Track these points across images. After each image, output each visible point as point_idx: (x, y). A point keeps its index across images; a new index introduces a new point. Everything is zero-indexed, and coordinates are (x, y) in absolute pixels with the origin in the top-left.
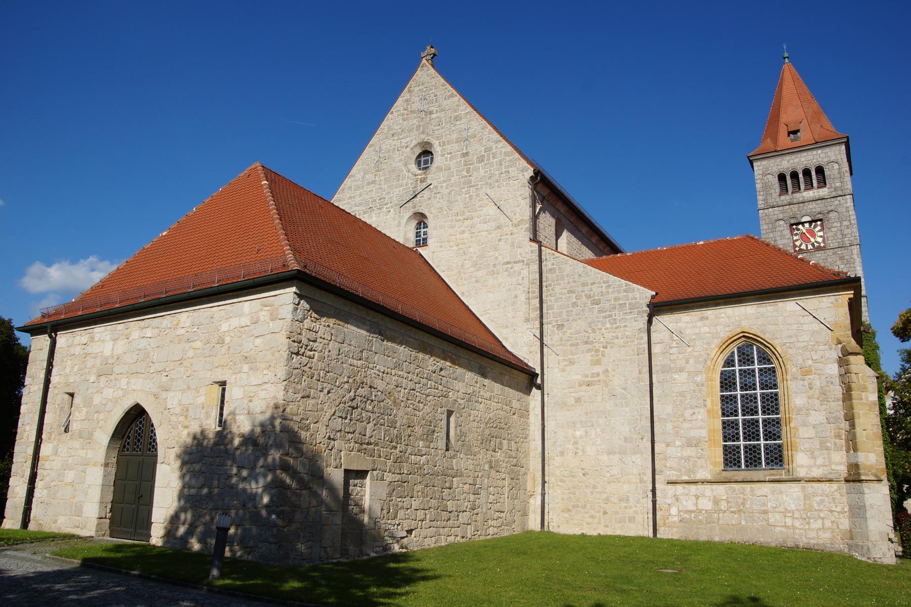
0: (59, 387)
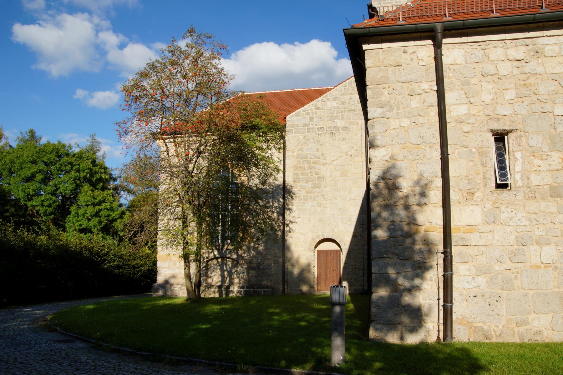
0: (472, 120)
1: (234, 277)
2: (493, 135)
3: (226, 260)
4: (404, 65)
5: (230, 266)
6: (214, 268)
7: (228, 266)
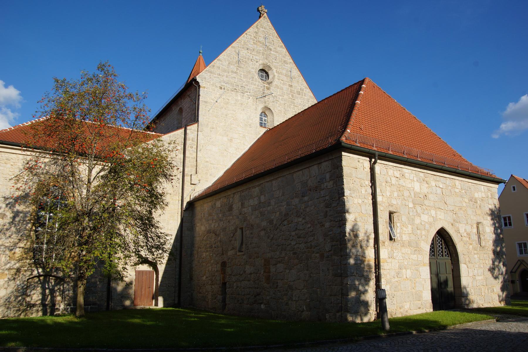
1: (56, 294)
2: (389, 213)
3: (49, 279)
4: (358, 169)
5: (53, 284)
6: (35, 286)
7: (50, 284)
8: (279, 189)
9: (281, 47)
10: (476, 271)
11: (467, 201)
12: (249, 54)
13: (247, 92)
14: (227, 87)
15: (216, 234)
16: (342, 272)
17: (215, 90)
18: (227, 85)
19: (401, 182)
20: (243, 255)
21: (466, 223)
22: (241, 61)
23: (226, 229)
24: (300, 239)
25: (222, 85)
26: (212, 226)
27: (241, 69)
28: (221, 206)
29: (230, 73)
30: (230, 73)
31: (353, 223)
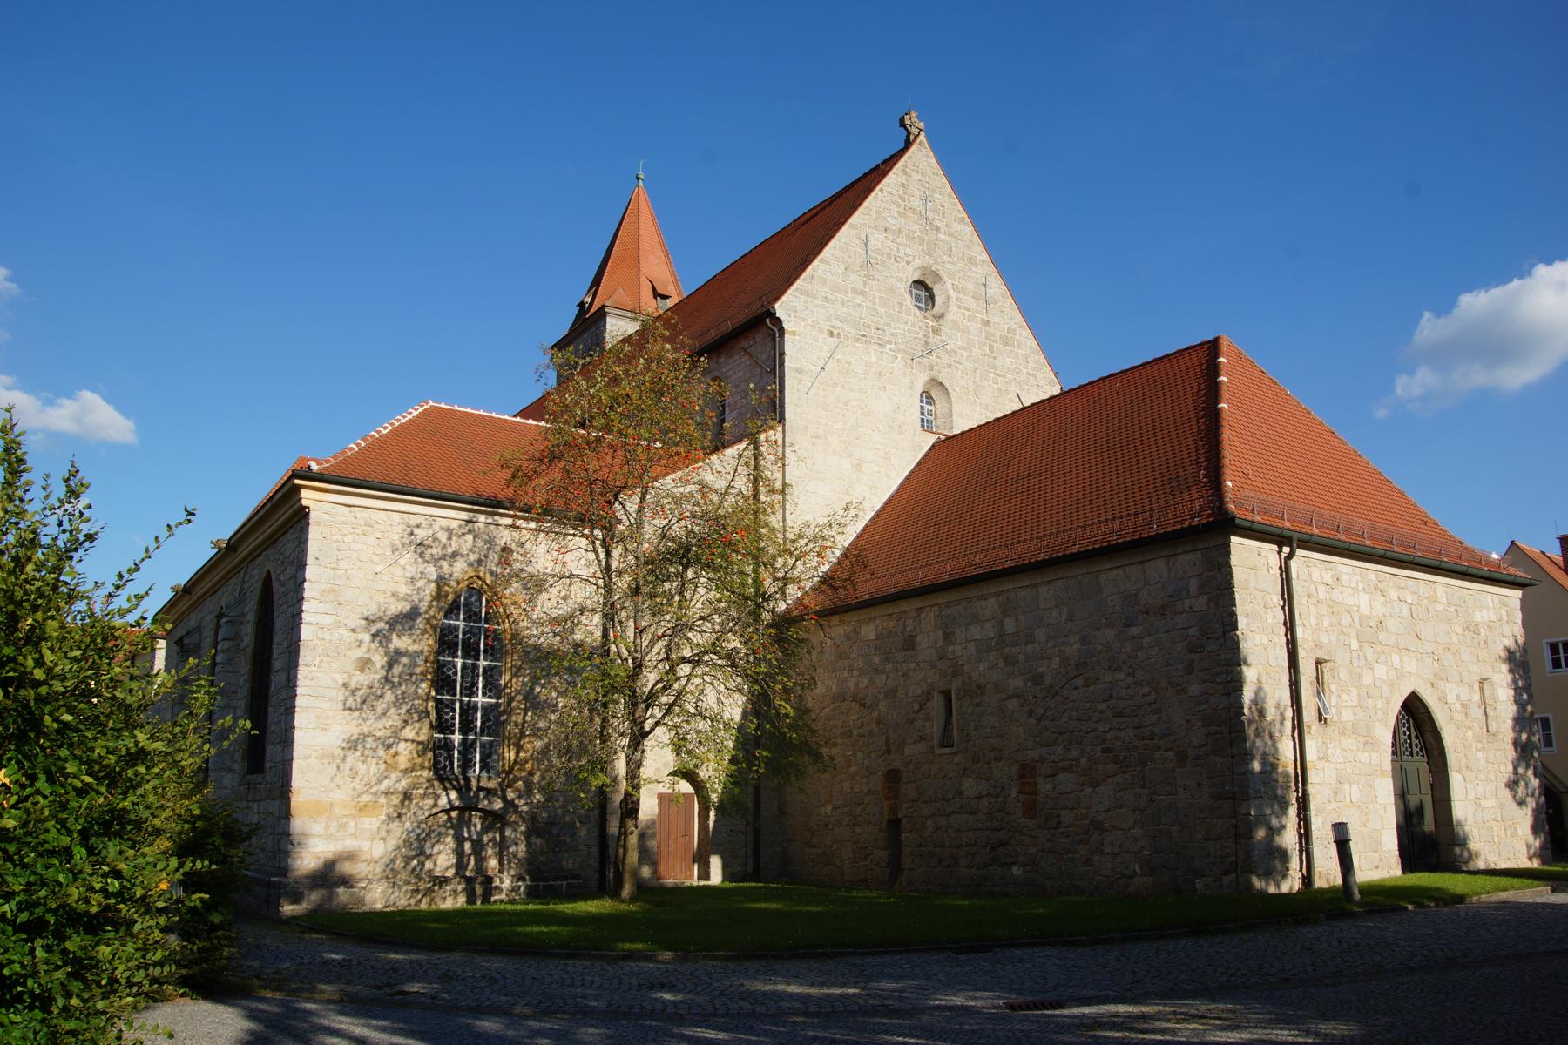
3: (471, 816)
5: (479, 827)
6: (440, 834)
7: (473, 829)
8: (1056, 606)
9: (961, 221)
10: (1480, 788)
11: (1459, 629)
12: (889, 243)
13: (890, 343)
14: (843, 331)
15: (863, 705)
16: (1236, 789)
17: (817, 341)
18: (844, 325)
19: (1335, 594)
20: (955, 754)
21: (1458, 679)
22: (872, 261)
23: (896, 691)
24: (1121, 719)
25: (833, 326)
26: (851, 685)
27: (873, 283)
28: (878, 637)
29: (850, 295)
30: (850, 295)
31: (1254, 687)
